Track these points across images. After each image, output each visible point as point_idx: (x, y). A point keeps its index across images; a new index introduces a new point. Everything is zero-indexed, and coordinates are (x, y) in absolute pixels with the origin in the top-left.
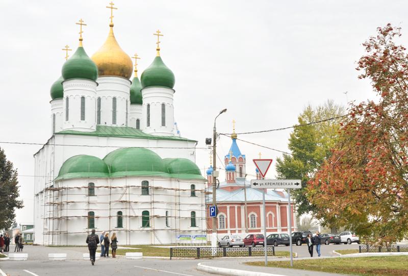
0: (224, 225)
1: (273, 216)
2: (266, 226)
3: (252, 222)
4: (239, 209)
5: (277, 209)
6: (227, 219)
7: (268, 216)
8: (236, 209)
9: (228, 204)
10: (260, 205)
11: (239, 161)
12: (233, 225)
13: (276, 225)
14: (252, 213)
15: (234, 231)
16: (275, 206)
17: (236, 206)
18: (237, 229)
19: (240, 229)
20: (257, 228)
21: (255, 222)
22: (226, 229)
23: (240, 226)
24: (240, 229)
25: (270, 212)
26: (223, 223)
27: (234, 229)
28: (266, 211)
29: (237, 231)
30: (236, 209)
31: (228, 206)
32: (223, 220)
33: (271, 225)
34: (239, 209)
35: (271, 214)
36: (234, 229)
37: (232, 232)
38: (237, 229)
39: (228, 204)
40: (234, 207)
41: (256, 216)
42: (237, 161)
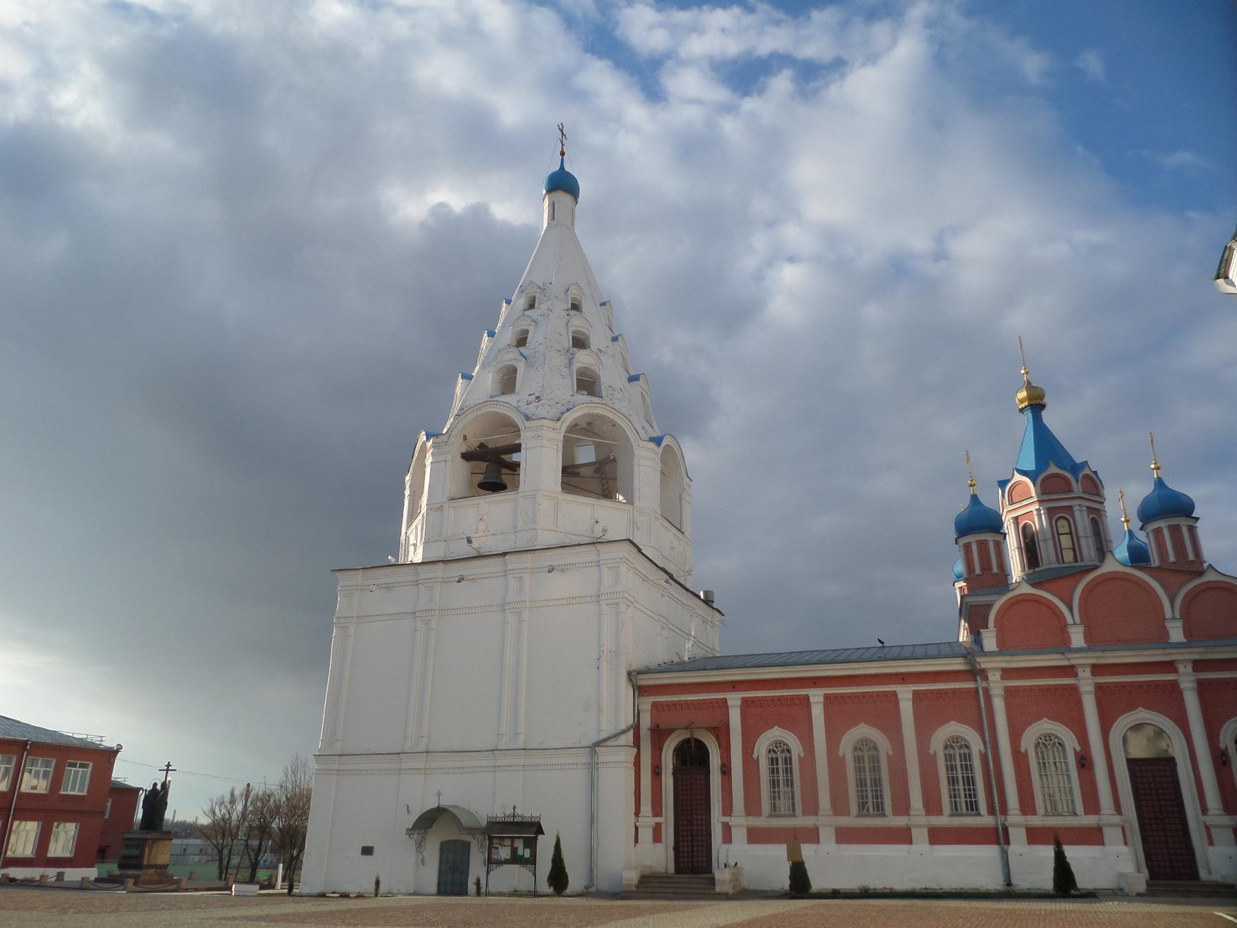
20: (985, 820)
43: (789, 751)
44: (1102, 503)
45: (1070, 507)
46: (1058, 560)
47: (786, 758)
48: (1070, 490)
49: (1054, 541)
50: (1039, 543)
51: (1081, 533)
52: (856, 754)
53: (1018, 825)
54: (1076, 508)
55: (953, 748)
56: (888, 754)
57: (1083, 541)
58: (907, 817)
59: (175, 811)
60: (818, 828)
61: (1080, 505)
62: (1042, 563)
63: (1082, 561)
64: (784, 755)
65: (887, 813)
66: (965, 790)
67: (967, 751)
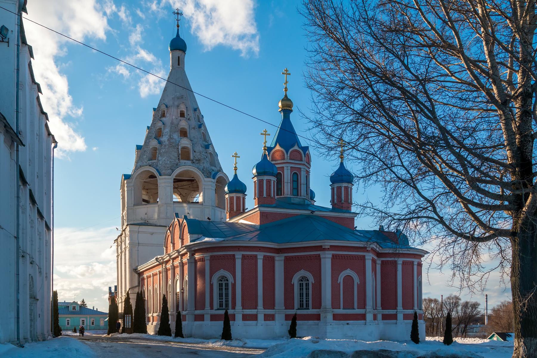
0: (227, 301)
2: (335, 304)
3: (301, 295)
4: (269, 263)
5: (369, 264)
6: (234, 285)
7: (341, 279)
8: (260, 263)
9: (239, 248)
13: (363, 304)
14: (302, 273)
15: (254, 318)
16: (363, 258)
17: (260, 256)
18: (261, 311)
19: (269, 312)
20: (311, 311)
21: (307, 295)
23: (269, 303)
24: (269, 312)
25: (348, 272)
26: (227, 295)
27: (253, 312)
28: (336, 270)
29: (261, 317)
30: (260, 263)
31: (239, 255)
32: (227, 289)
33: (349, 305)
34: (269, 263)
35: (349, 280)
36: (253, 312)
37: (245, 318)
38: (261, 311)
39: (239, 248)
40: (256, 256)
41: (311, 280)
43: (227, 280)
44: (310, 168)
45: (300, 168)
46: (291, 193)
47: (226, 283)
48: (301, 160)
49: (291, 183)
50: (284, 184)
52: (219, 282)
54: (302, 169)
55: (221, 281)
56: (232, 283)
57: (302, 186)
60: (235, 315)
61: (304, 169)
62: (284, 193)
63: (300, 196)
64: (225, 282)
66: (303, 299)
67: (227, 282)
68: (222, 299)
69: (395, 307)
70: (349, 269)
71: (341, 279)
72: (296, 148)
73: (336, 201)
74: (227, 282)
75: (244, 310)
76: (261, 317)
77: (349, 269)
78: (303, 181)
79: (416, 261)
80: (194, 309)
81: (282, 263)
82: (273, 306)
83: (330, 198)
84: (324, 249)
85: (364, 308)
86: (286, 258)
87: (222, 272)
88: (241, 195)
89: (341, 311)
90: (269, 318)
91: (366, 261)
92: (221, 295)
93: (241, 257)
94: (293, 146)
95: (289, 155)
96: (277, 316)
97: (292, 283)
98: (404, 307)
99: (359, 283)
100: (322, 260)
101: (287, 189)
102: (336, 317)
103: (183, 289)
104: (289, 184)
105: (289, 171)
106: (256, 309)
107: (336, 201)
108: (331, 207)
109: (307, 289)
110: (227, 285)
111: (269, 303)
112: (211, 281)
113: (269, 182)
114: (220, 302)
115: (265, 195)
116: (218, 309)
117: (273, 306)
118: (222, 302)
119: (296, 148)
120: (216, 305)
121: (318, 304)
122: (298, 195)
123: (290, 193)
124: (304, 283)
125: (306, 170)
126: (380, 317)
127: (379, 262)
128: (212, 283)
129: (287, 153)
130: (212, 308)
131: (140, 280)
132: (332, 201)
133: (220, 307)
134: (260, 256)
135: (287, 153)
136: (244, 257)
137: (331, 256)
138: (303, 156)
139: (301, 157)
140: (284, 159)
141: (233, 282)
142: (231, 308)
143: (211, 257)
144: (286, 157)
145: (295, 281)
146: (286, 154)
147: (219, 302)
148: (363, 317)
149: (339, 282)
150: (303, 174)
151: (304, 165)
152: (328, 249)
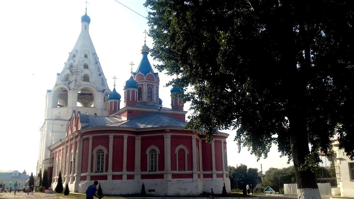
1: (187, 152)
2: (173, 168)
6: (107, 156)
10: (164, 134)
11: (147, 79)
12: (118, 166)
13: (191, 168)
14: (153, 147)
15: (120, 177)
17: (126, 136)
18: (125, 172)
20: (158, 172)
21: (156, 162)
22: (104, 173)
23: (131, 167)
25: (181, 146)
28: (174, 145)
29: (125, 177)
31: (111, 136)
33: (182, 168)
35: (182, 151)
37: (114, 177)
38: (125, 172)
40: (123, 136)
42: (145, 78)
43: (103, 152)
45: (153, 85)
47: (102, 154)
48: (154, 80)
51: (154, 93)
53: (196, 173)
54: (154, 86)
57: (154, 95)
58: (192, 171)
59: (261, 165)
65: (186, 170)
68: (99, 165)
69: (211, 169)
70: (182, 145)
71: (177, 151)
72: (150, 73)
73: (174, 104)
74: (103, 154)
75: (114, 173)
76: (125, 177)
77: (182, 145)
78: (155, 92)
79: (223, 140)
80: (81, 172)
81: (140, 141)
82: (133, 170)
83: (170, 103)
84: (166, 132)
85: (192, 170)
86: (142, 137)
87: (100, 147)
88: (117, 101)
89: (177, 172)
90: (130, 177)
91: (193, 140)
92: (98, 163)
93: (113, 137)
94: (148, 72)
95: (146, 77)
96: (136, 177)
97: (146, 154)
98: (217, 170)
99: (188, 153)
100: (165, 139)
101: (145, 97)
102: (174, 176)
103: (75, 159)
104: (146, 94)
105: (146, 86)
106: (122, 171)
107: (174, 104)
108: (171, 108)
109: (156, 158)
110: (103, 155)
111: (131, 167)
112: (92, 153)
113: (133, 92)
114: (98, 167)
115: (131, 100)
116: (96, 172)
117: (133, 170)
118: (99, 167)
119: (150, 73)
120: (95, 169)
121: (162, 167)
122: (151, 101)
123: (146, 99)
124: (154, 154)
125: (157, 86)
126: (202, 176)
127: (200, 141)
128: (93, 154)
129: (145, 76)
130: (92, 171)
131: (51, 154)
132: (172, 105)
133: (98, 170)
134: (126, 136)
135: (145, 76)
136: (115, 137)
137: (170, 136)
138: (155, 78)
139: (154, 79)
140: (143, 79)
141: (107, 154)
142: (105, 171)
143: (93, 137)
144: (144, 78)
145: (148, 152)
146: (144, 76)
147: (97, 167)
148: (191, 176)
149: (175, 153)
150: (155, 88)
151: (155, 83)
152: (169, 132)
